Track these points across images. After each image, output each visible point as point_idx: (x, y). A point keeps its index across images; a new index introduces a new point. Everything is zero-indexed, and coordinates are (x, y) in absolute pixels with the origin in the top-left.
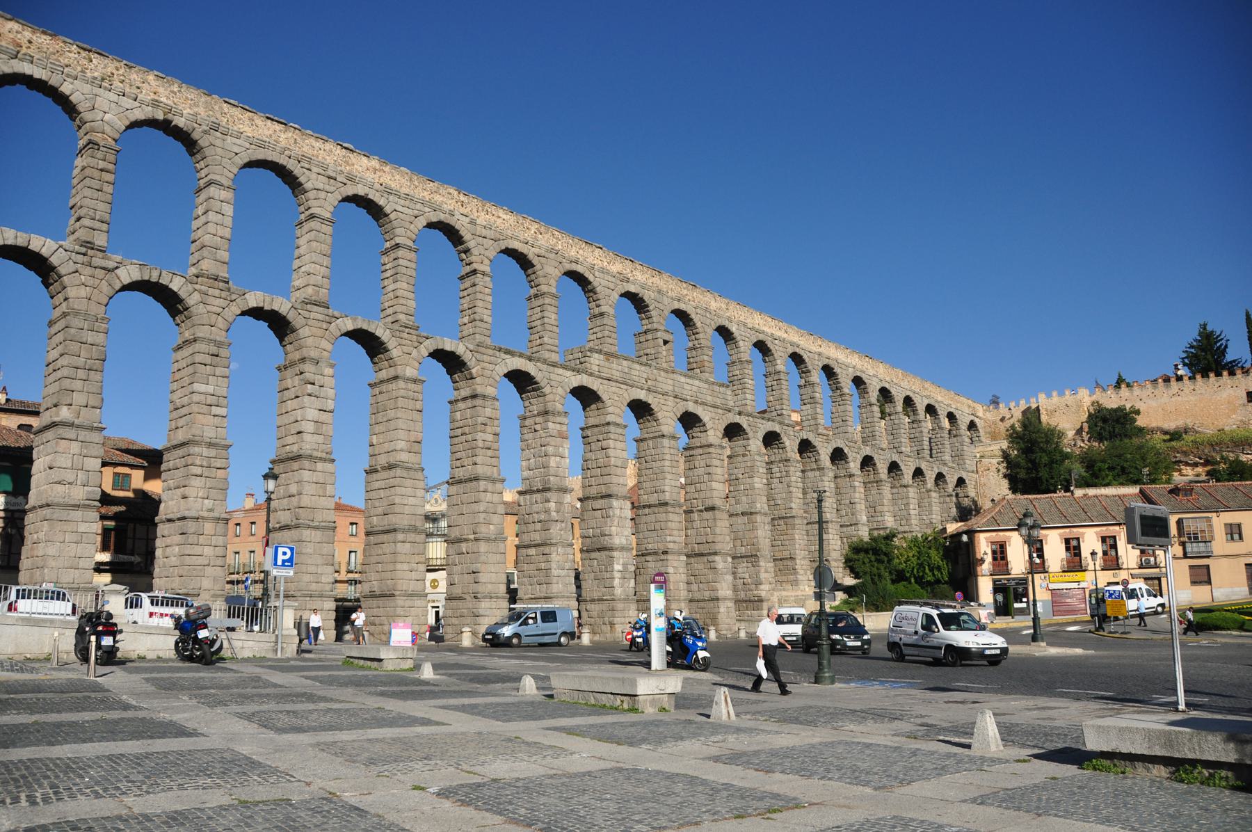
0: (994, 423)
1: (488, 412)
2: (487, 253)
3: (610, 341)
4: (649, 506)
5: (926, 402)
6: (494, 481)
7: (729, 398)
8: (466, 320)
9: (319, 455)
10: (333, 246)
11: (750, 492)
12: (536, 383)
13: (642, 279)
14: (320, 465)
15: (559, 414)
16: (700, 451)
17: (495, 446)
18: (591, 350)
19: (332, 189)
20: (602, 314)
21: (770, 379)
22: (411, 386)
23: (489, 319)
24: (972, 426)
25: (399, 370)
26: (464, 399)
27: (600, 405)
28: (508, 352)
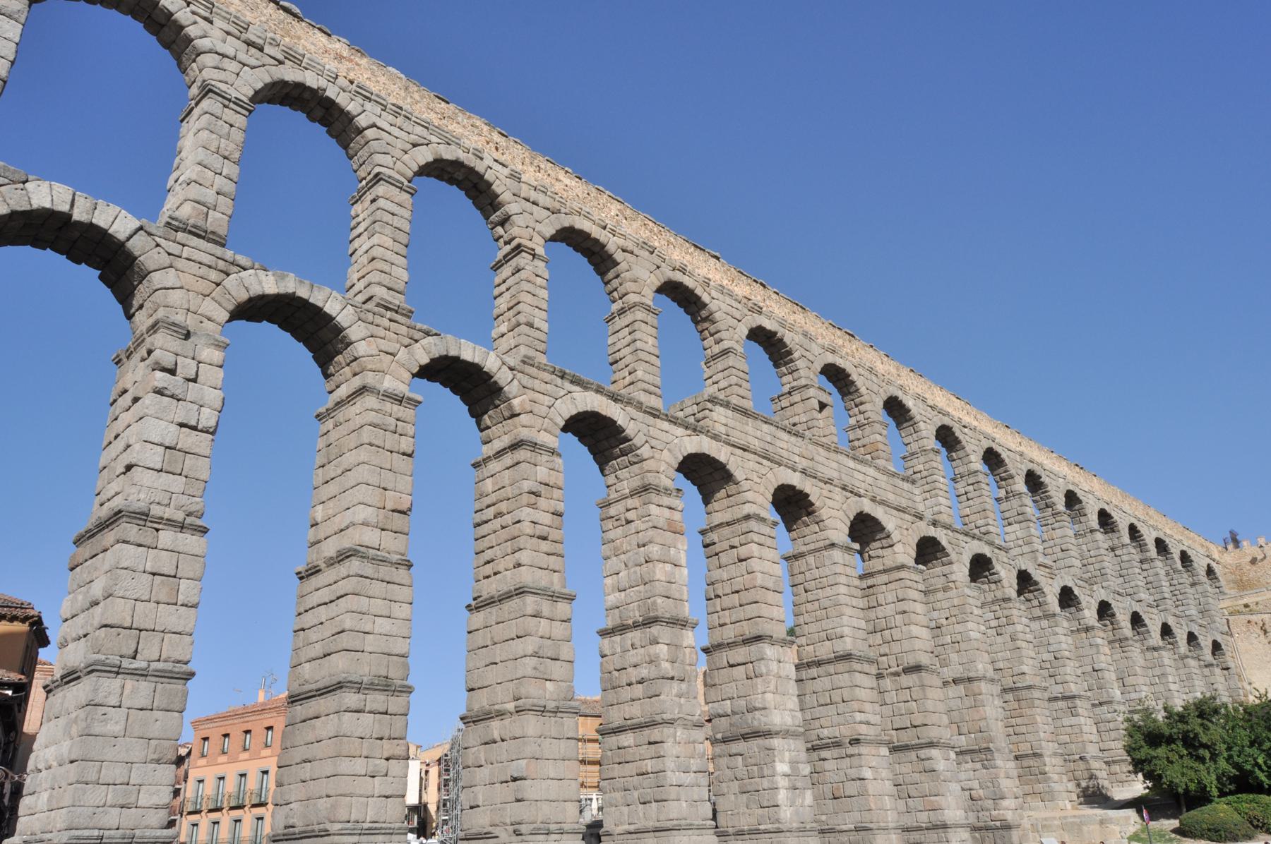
0: (1239, 567)
1: (542, 473)
2: (538, 227)
3: (741, 391)
4: (819, 664)
5: (1155, 535)
6: (554, 597)
7: (918, 499)
8: (504, 328)
9: (168, 513)
10: (246, 147)
11: (963, 646)
12: (627, 440)
13: (777, 313)
14: (167, 537)
15: (667, 492)
16: (884, 578)
17: (555, 535)
18: (713, 400)
19: (253, 62)
20: (725, 352)
21: (963, 483)
22: (389, 406)
23: (545, 327)
24: (1210, 571)
25: (369, 379)
26: (500, 454)
27: (731, 488)
28: (575, 381)
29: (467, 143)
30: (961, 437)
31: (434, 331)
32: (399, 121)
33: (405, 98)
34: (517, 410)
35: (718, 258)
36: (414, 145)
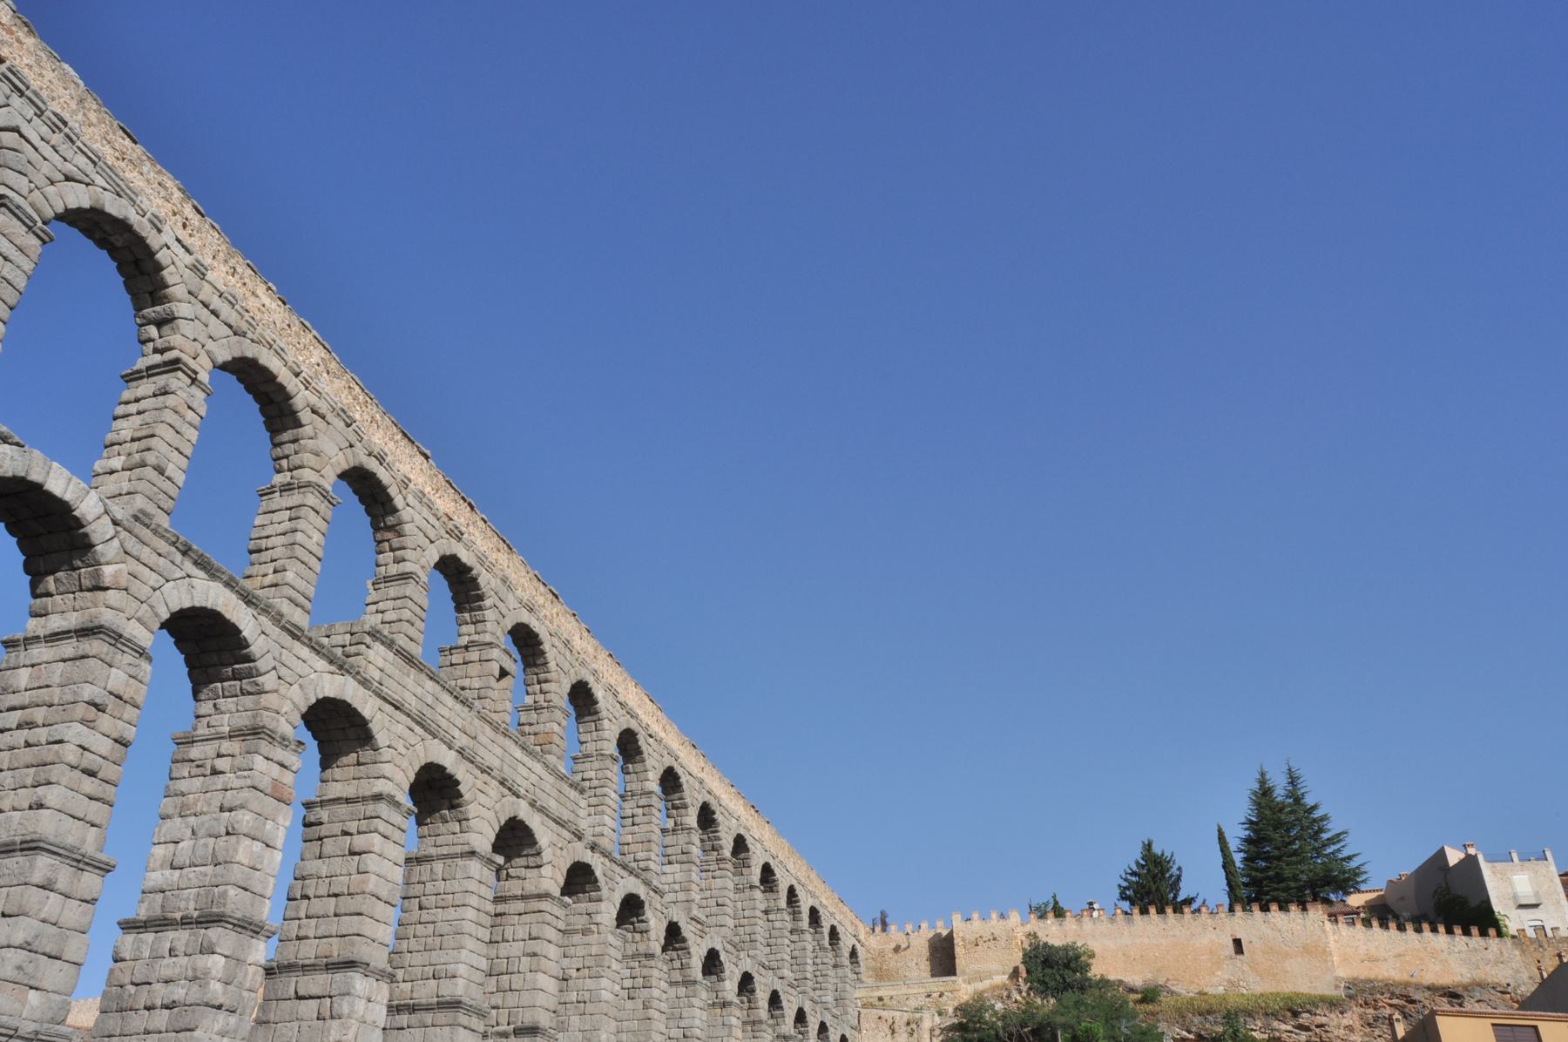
0: (882, 954)
1: (117, 678)
2: (210, 345)
3: (412, 631)
4: (413, 1009)
5: (811, 902)
6: (81, 862)
7: (582, 813)
8: (117, 463)
11: (590, 1008)
12: (249, 659)
13: (480, 547)
15: (284, 742)
16: (519, 906)
17: (109, 771)
18: (374, 634)
20: (405, 577)
21: (631, 803)
23: (180, 478)
24: (853, 954)
26: (56, 637)
27: (366, 755)
28: (202, 563)
29: (145, 205)
30: (644, 747)
31: (17, 439)
32: (57, 138)
33: (74, 112)
34: (107, 581)
35: (427, 458)
36: (68, 179)
